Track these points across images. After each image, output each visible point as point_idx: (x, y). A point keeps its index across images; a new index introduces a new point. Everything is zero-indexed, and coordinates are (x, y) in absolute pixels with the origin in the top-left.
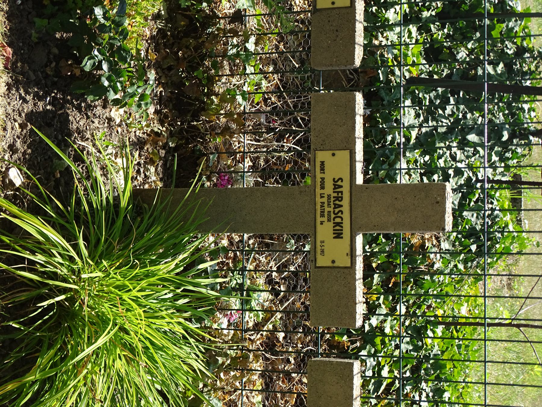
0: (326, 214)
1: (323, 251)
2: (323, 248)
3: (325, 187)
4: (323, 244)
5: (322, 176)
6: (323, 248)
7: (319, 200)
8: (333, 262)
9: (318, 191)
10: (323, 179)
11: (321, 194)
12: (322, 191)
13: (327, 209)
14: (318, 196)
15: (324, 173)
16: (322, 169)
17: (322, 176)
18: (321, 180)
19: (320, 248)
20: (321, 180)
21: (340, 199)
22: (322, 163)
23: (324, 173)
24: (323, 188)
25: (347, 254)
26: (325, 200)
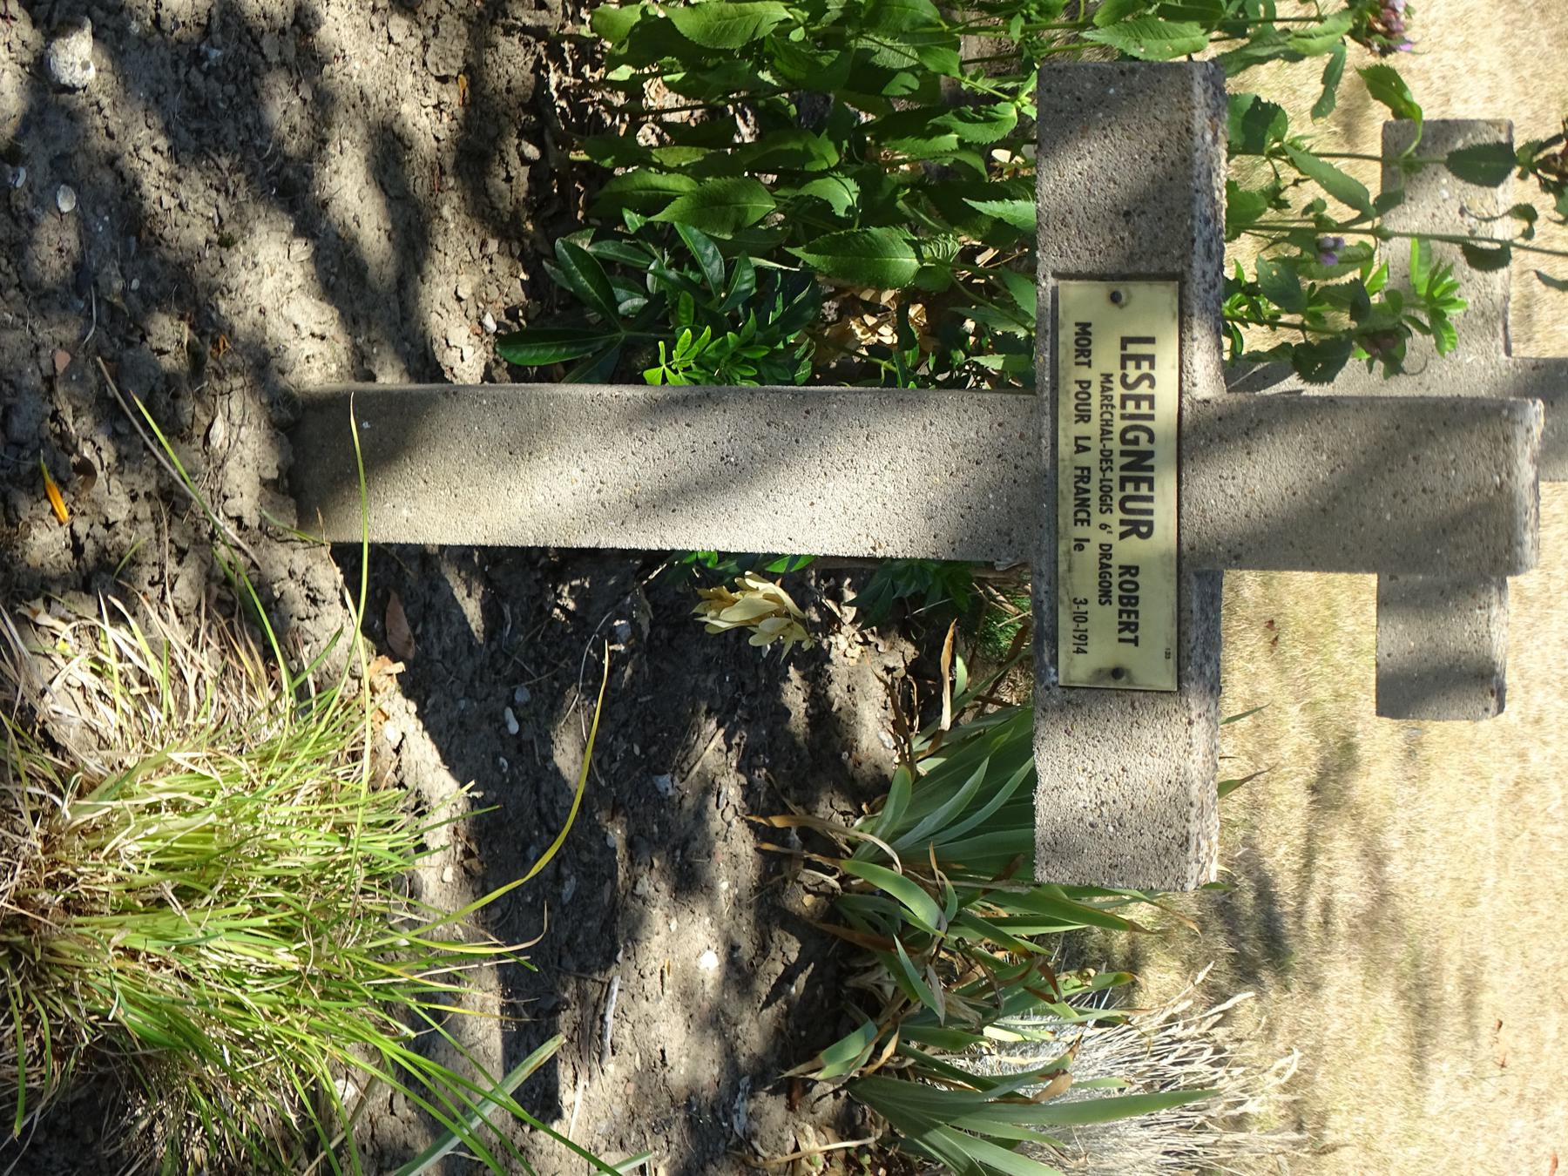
1: (1083, 637)
2: (1082, 627)
5: (1084, 373)
6: (1082, 627)
9: (1069, 430)
10: (1085, 385)
11: (1077, 438)
12: (1082, 429)
14: (1066, 448)
15: (1089, 364)
19: (1073, 625)
20: (1077, 388)
24: (1084, 417)
26: (1091, 459)
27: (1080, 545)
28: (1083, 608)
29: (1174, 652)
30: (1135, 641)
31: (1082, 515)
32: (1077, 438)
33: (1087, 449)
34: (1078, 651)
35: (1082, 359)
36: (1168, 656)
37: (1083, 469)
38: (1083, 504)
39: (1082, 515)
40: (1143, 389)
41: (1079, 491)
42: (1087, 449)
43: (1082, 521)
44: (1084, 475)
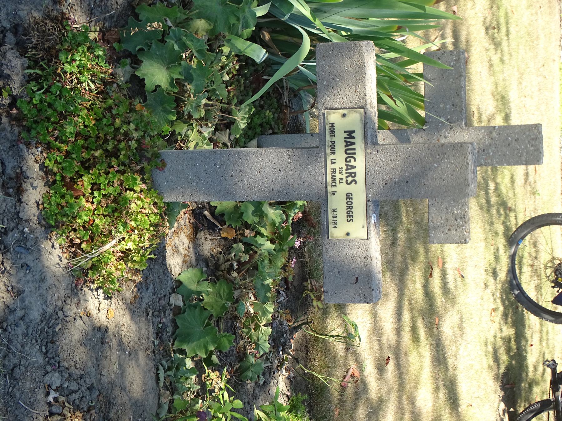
0: (338, 182)
1: (335, 223)
2: (335, 219)
6: (335, 219)
7: (330, 167)
8: (348, 234)
10: (333, 143)
12: (332, 157)
13: (338, 176)
14: (329, 162)
15: (334, 136)
16: (332, 132)
20: (331, 144)
22: (332, 125)
24: (333, 153)
28: (335, 213)
33: (335, 163)
35: (332, 134)
36: (363, 227)
37: (333, 169)
38: (334, 180)
39: (334, 184)
41: (333, 176)
42: (335, 163)
43: (334, 186)
44: (334, 171)
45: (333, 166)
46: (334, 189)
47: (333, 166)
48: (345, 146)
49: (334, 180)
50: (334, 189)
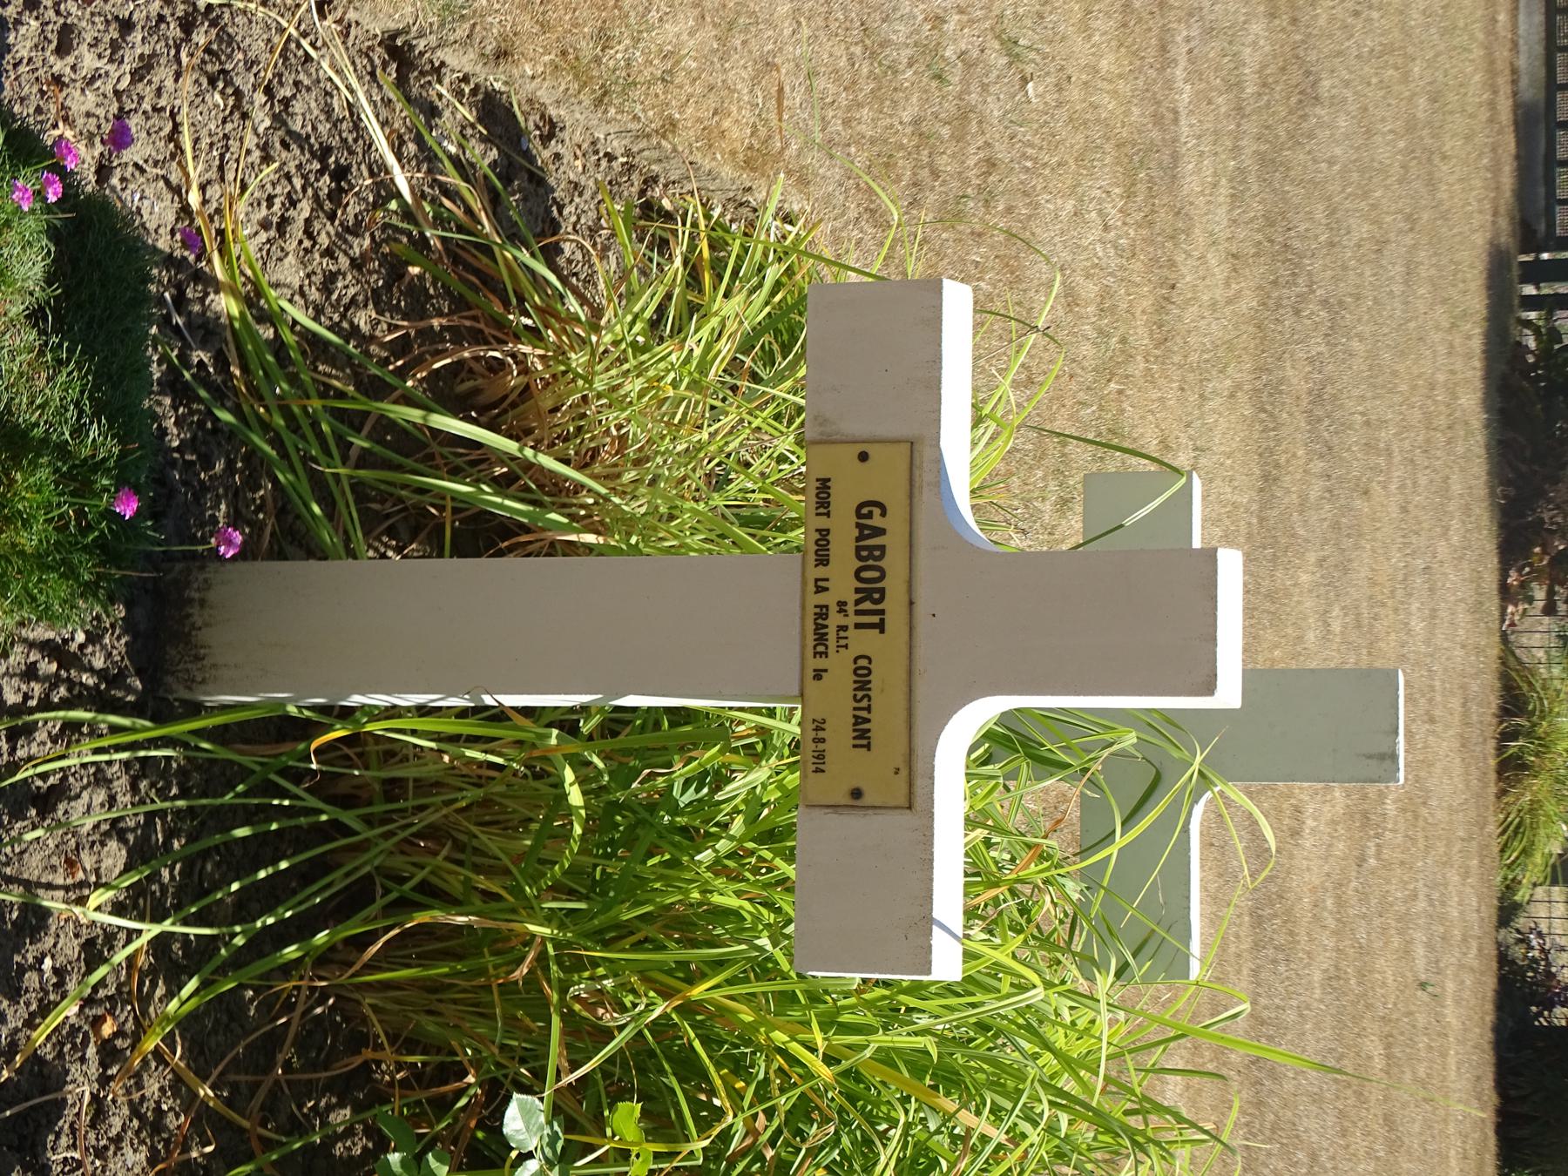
3: (831, 559)
4: (821, 734)
5: (823, 522)
6: (821, 746)
10: (824, 533)
11: (817, 580)
12: (821, 572)
15: (828, 515)
17: (823, 522)
18: (817, 536)
19: (813, 746)
20: (817, 536)
21: (876, 596)
23: (828, 515)
24: (823, 561)
25: (897, 771)
27: (818, 675)
29: (904, 772)
30: (868, 747)
31: (821, 649)
32: (817, 580)
34: (817, 771)
35: (822, 510)
37: (821, 607)
38: (821, 638)
39: (821, 649)
40: (877, 521)
41: (818, 627)
43: (821, 654)
44: (822, 612)
45: (822, 599)
46: (821, 663)
47: (822, 599)
48: (858, 539)
49: (821, 638)
50: (821, 663)
